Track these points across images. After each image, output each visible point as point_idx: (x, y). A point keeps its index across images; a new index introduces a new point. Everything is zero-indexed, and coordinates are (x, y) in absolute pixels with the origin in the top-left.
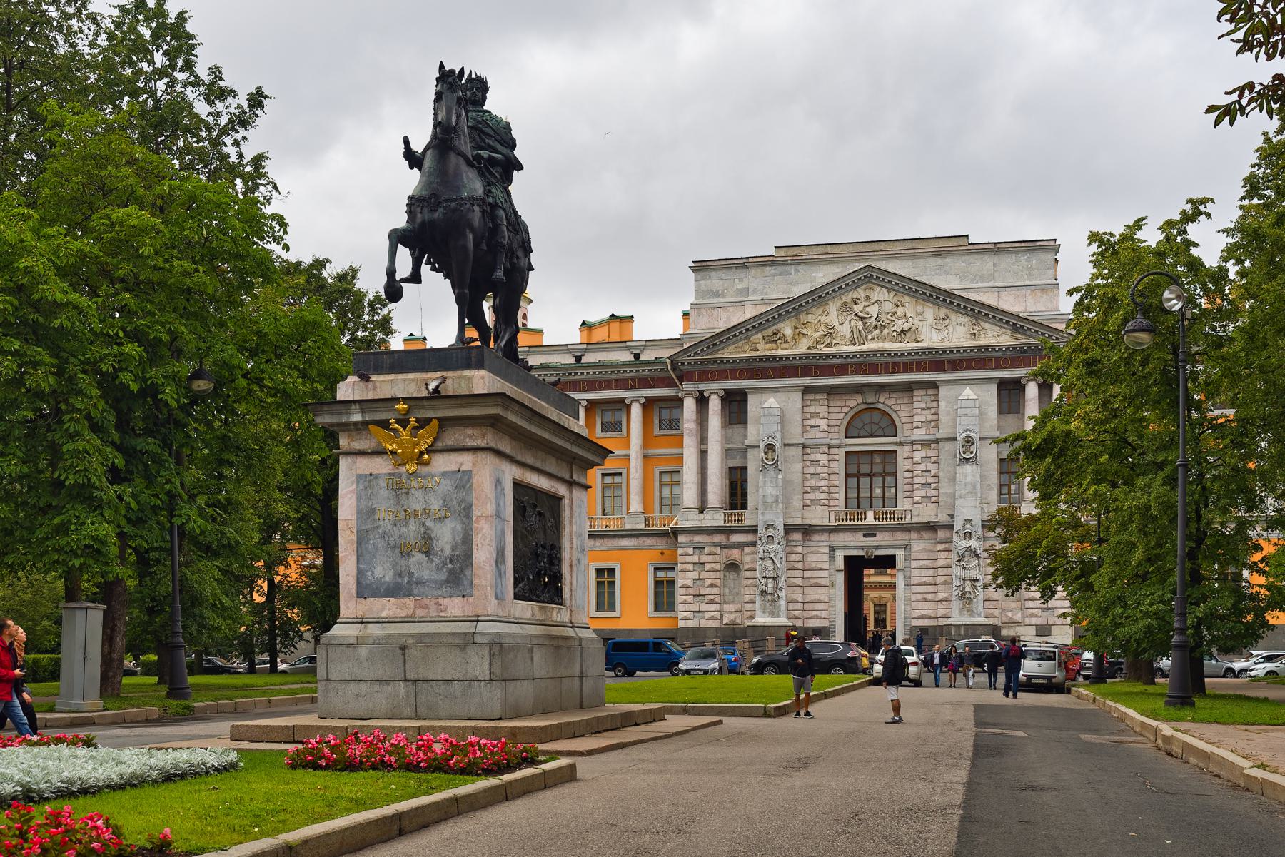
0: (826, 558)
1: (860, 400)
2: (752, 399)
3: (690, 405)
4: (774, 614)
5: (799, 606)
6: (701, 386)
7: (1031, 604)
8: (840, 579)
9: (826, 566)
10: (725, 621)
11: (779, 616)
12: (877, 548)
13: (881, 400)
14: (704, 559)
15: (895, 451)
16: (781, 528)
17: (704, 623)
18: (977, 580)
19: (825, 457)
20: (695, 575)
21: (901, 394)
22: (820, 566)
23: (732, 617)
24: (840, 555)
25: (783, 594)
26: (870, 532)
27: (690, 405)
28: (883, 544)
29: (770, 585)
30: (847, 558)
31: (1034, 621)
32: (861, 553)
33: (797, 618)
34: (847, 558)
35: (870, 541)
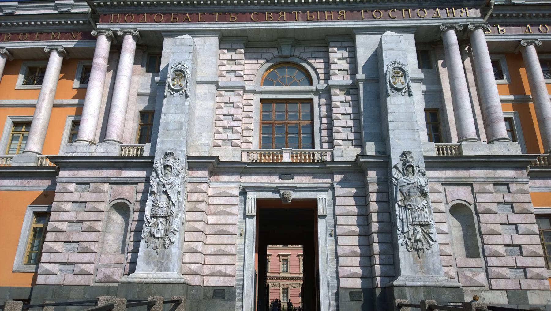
0: (236, 200)
1: (276, 53)
2: (168, 44)
3: (103, 45)
4: (163, 266)
5: (198, 257)
6: (117, 27)
7: (492, 261)
8: (251, 225)
9: (234, 210)
10: (100, 277)
11: (167, 269)
12: (296, 189)
13: (297, 53)
14: (88, 196)
15: (311, 100)
16: (183, 158)
17: (70, 279)
18: (427, 225)
19: (240, 99)
20: (71, 216)
21: (316, 49)
22: (229, 210)
23: (108, 271)
24: (252, 196)
25: (175, 239)
26: (287, 171)
27: (103, 45)
28: (302, 187)
29: (161, 226)
30: (260, 202)
31: (502, 284)
32: (277, 196)
33: (195, 274)
34: (260, 202)
35: (287, 183)
